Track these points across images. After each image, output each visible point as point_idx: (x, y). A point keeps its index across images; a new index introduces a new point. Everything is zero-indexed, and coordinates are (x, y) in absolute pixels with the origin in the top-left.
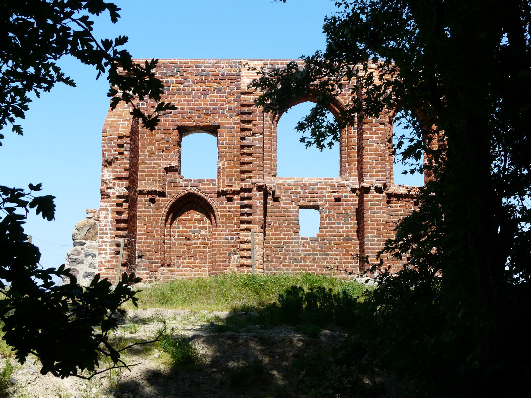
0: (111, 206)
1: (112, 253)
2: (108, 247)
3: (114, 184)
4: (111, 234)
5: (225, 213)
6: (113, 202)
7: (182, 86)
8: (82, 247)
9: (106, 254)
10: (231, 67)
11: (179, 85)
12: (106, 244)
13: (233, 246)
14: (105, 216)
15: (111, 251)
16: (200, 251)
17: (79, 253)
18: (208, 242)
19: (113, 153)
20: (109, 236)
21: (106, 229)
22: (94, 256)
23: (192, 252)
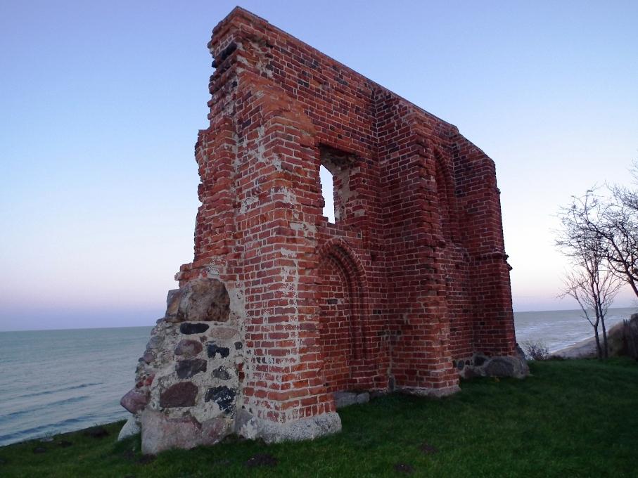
1: (303, 349)
2: (296, 338)
3: (301, 218)
4: (300, 311)
5: (371, 277)
6: (301, 248)
7: (320, 87)
8: (201, 335)
9: (296, 353)
10: (366, 86)
11: (318, 84)
12: (292, 331)
13: (381, 323)
14: (288, 274)
15: (302, 346)
16: (338, 331)
17: (198, 348)
18: (345, 316)
19: (295, 157)
20: (296, 314)
21: (292, 302)
22: (225, 352)
23: (330, 333)
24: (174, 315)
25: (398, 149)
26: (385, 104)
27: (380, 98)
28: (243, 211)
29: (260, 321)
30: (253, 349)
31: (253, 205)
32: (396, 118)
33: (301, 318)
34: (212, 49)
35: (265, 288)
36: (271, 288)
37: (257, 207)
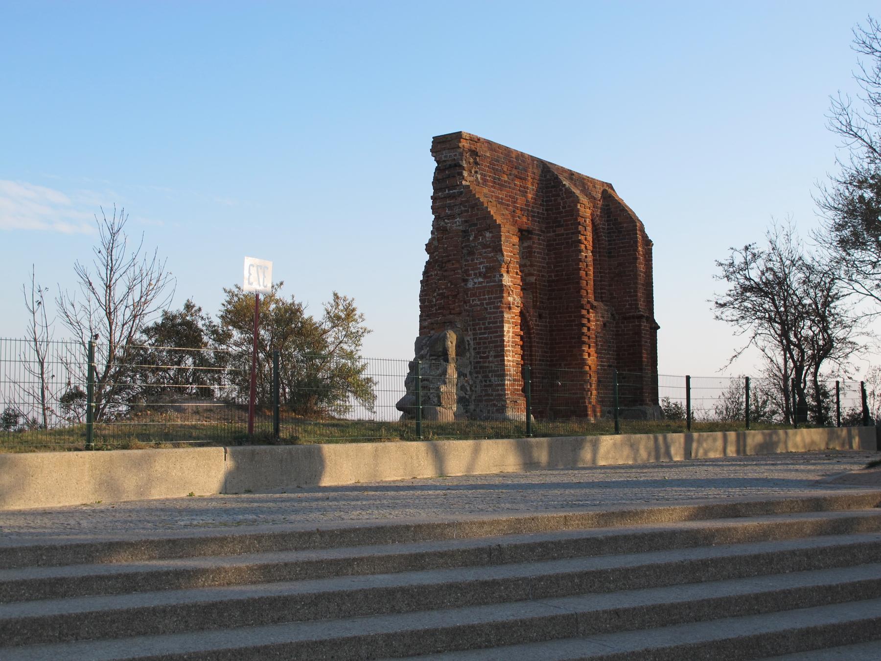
0: (513, 318)
24: (440, 351)
25: (562, 226)
26: (552, 183)
27: (548, 177)
28: (470, 285)
29: (487, 357)
30: (480, 376)
31: (480, 283)
32: (562, 199)
33: (513, 356)
34: (435, 154)
35: (491, 337)
36: (495, 337)
37: (484, 284)
